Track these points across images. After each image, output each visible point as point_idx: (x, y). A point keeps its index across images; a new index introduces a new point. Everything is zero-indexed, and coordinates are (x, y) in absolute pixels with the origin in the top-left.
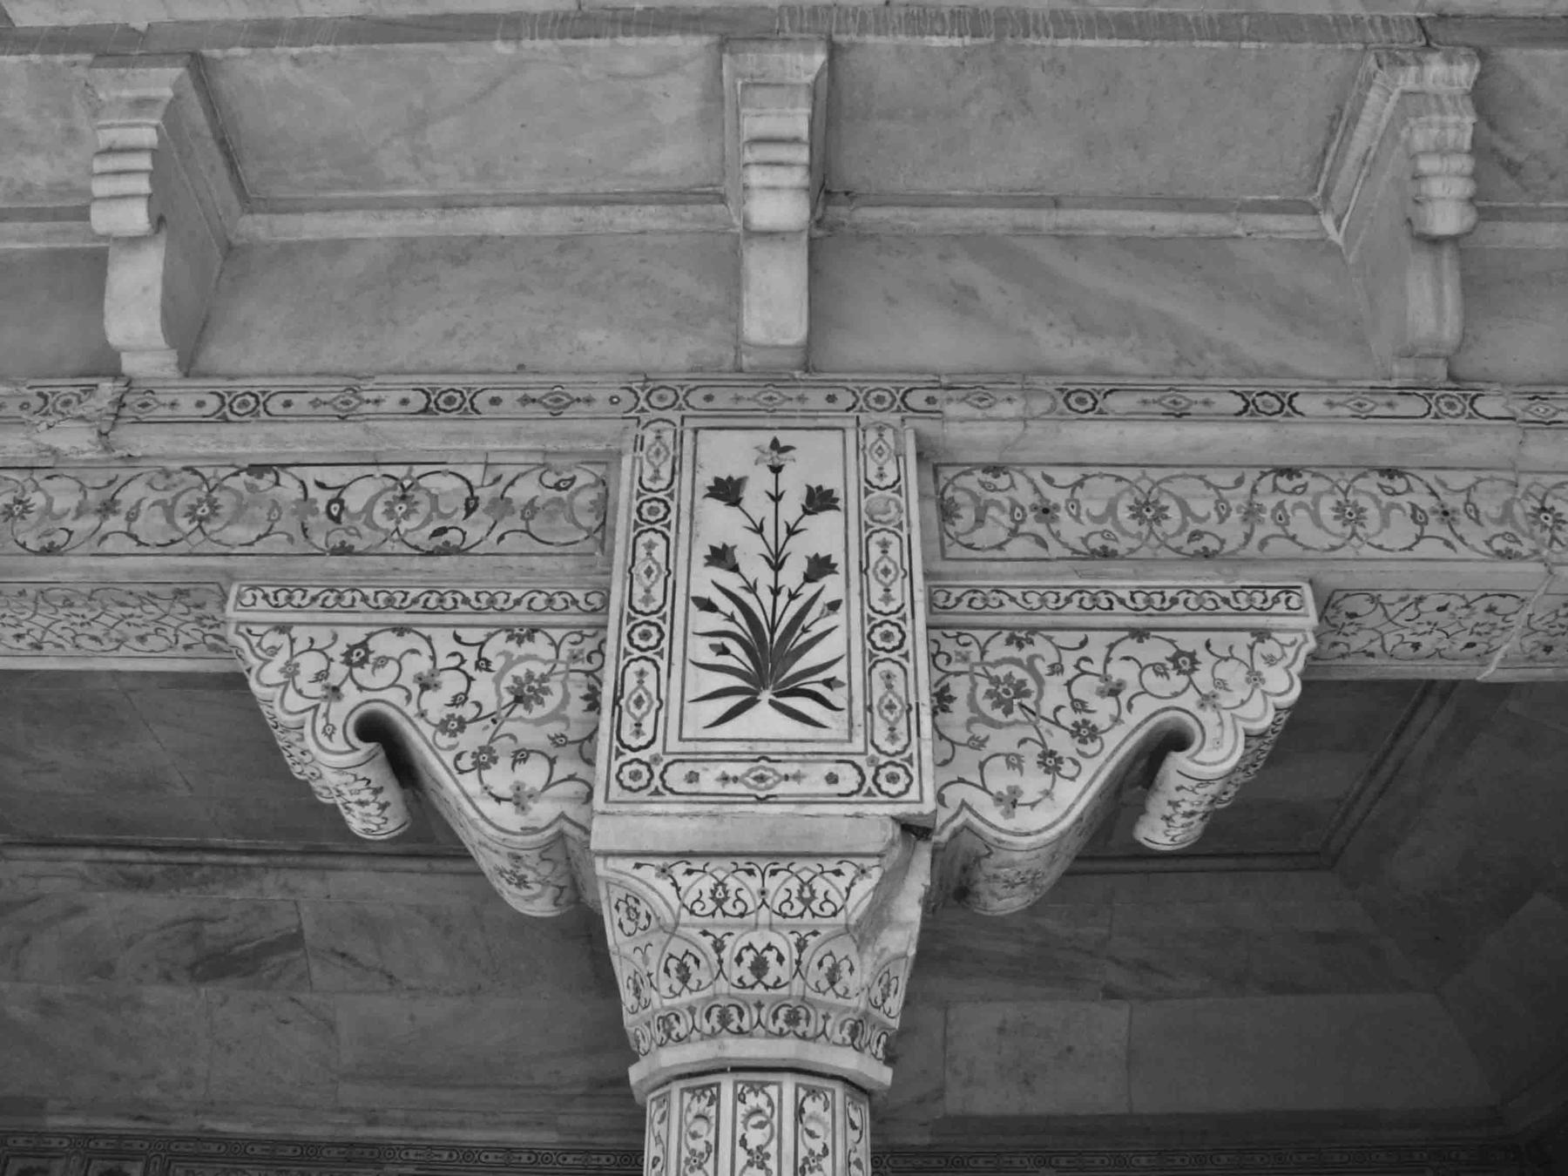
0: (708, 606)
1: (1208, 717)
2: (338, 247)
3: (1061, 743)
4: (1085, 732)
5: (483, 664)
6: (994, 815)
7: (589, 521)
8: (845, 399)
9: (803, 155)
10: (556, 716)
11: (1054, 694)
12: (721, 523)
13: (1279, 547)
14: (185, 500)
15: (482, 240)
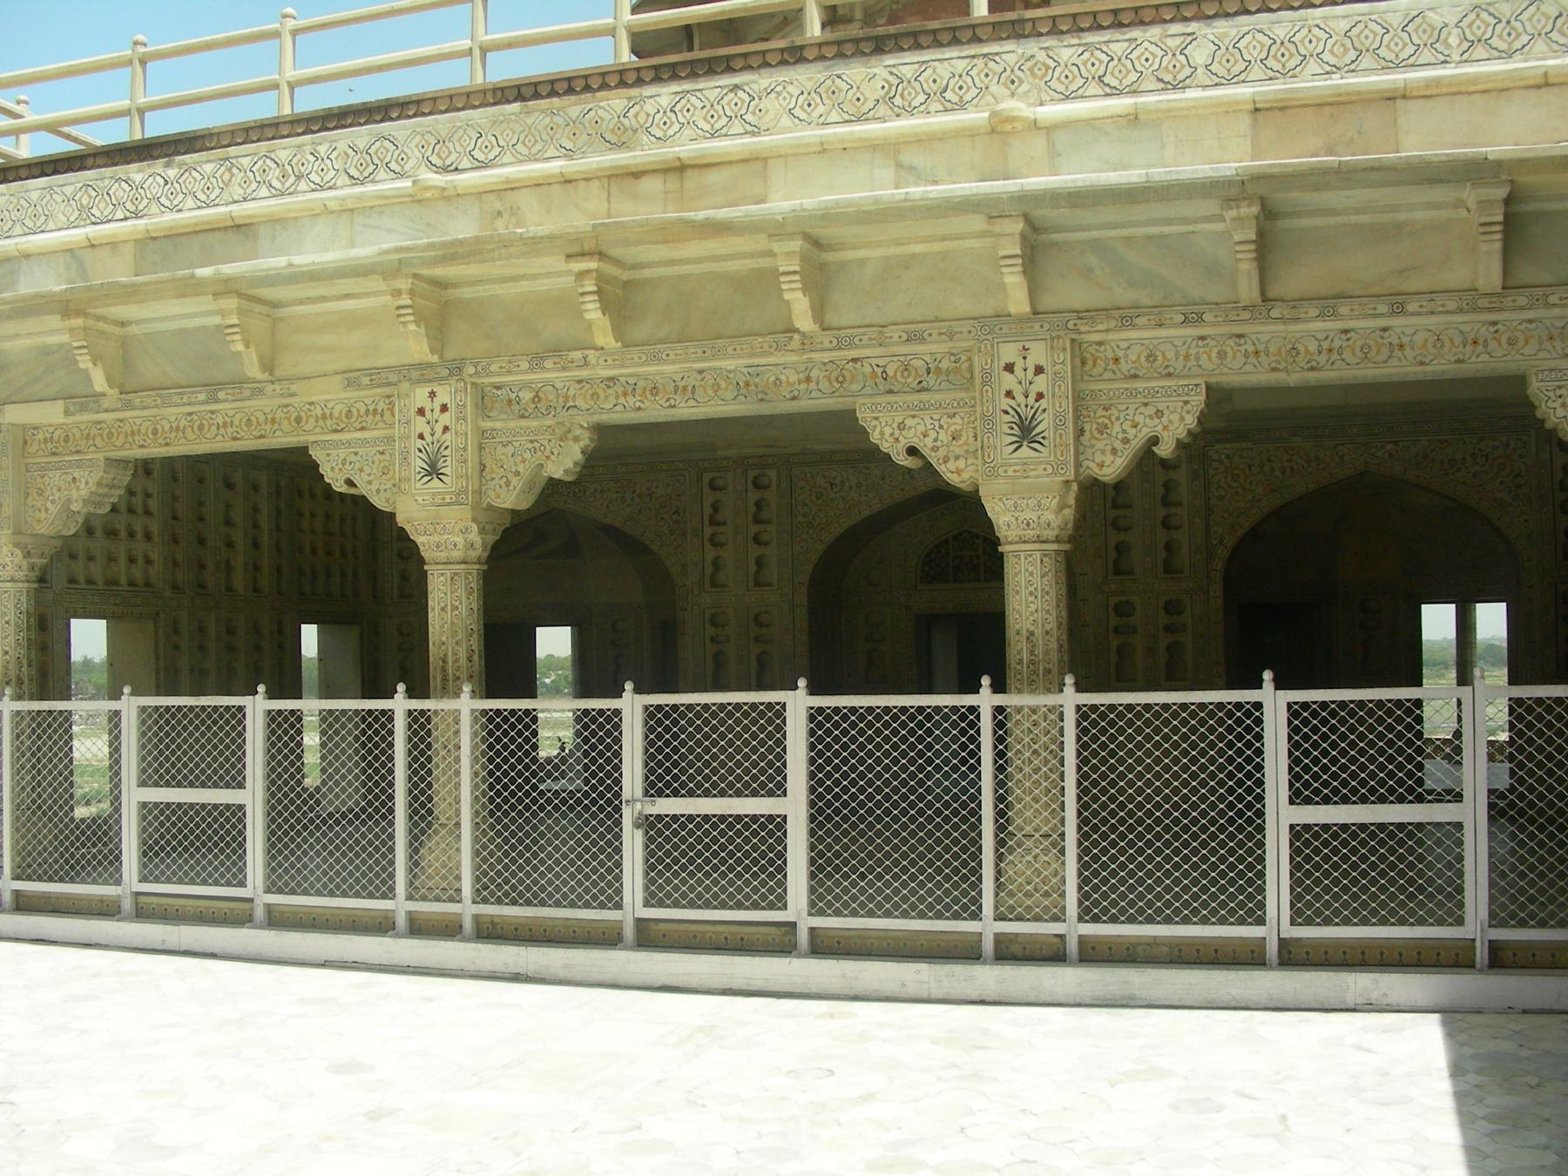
0: (1007, 413)
1: (1165, 434)
2: (862, 262)
3: (1118, 445)
4: (1126, 441)
5: (941, 427)
6: (1096, 470)
7: (967, 375)
8: (1046, 326)
9: (1020, 261)
10: (965, 444)
11: (1117, 428)
12: (1009, 381)
13: (1195, 370)
14: (834, 375)
15: (913, 255)
